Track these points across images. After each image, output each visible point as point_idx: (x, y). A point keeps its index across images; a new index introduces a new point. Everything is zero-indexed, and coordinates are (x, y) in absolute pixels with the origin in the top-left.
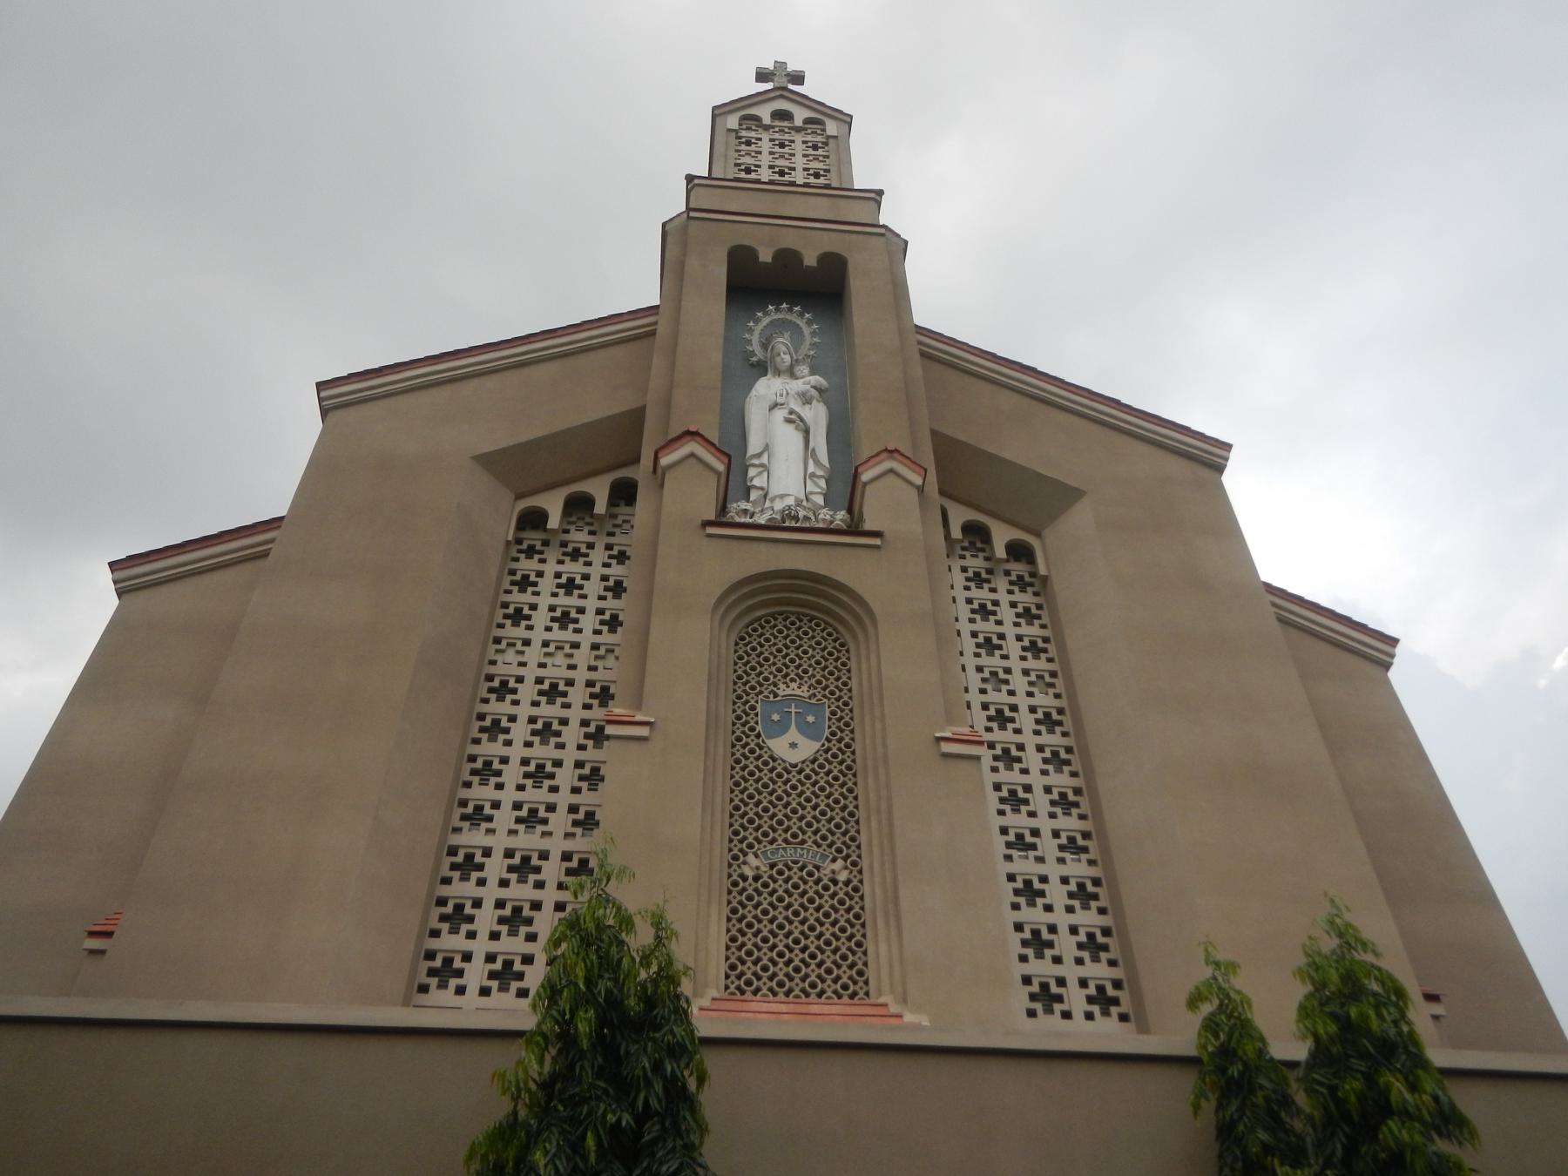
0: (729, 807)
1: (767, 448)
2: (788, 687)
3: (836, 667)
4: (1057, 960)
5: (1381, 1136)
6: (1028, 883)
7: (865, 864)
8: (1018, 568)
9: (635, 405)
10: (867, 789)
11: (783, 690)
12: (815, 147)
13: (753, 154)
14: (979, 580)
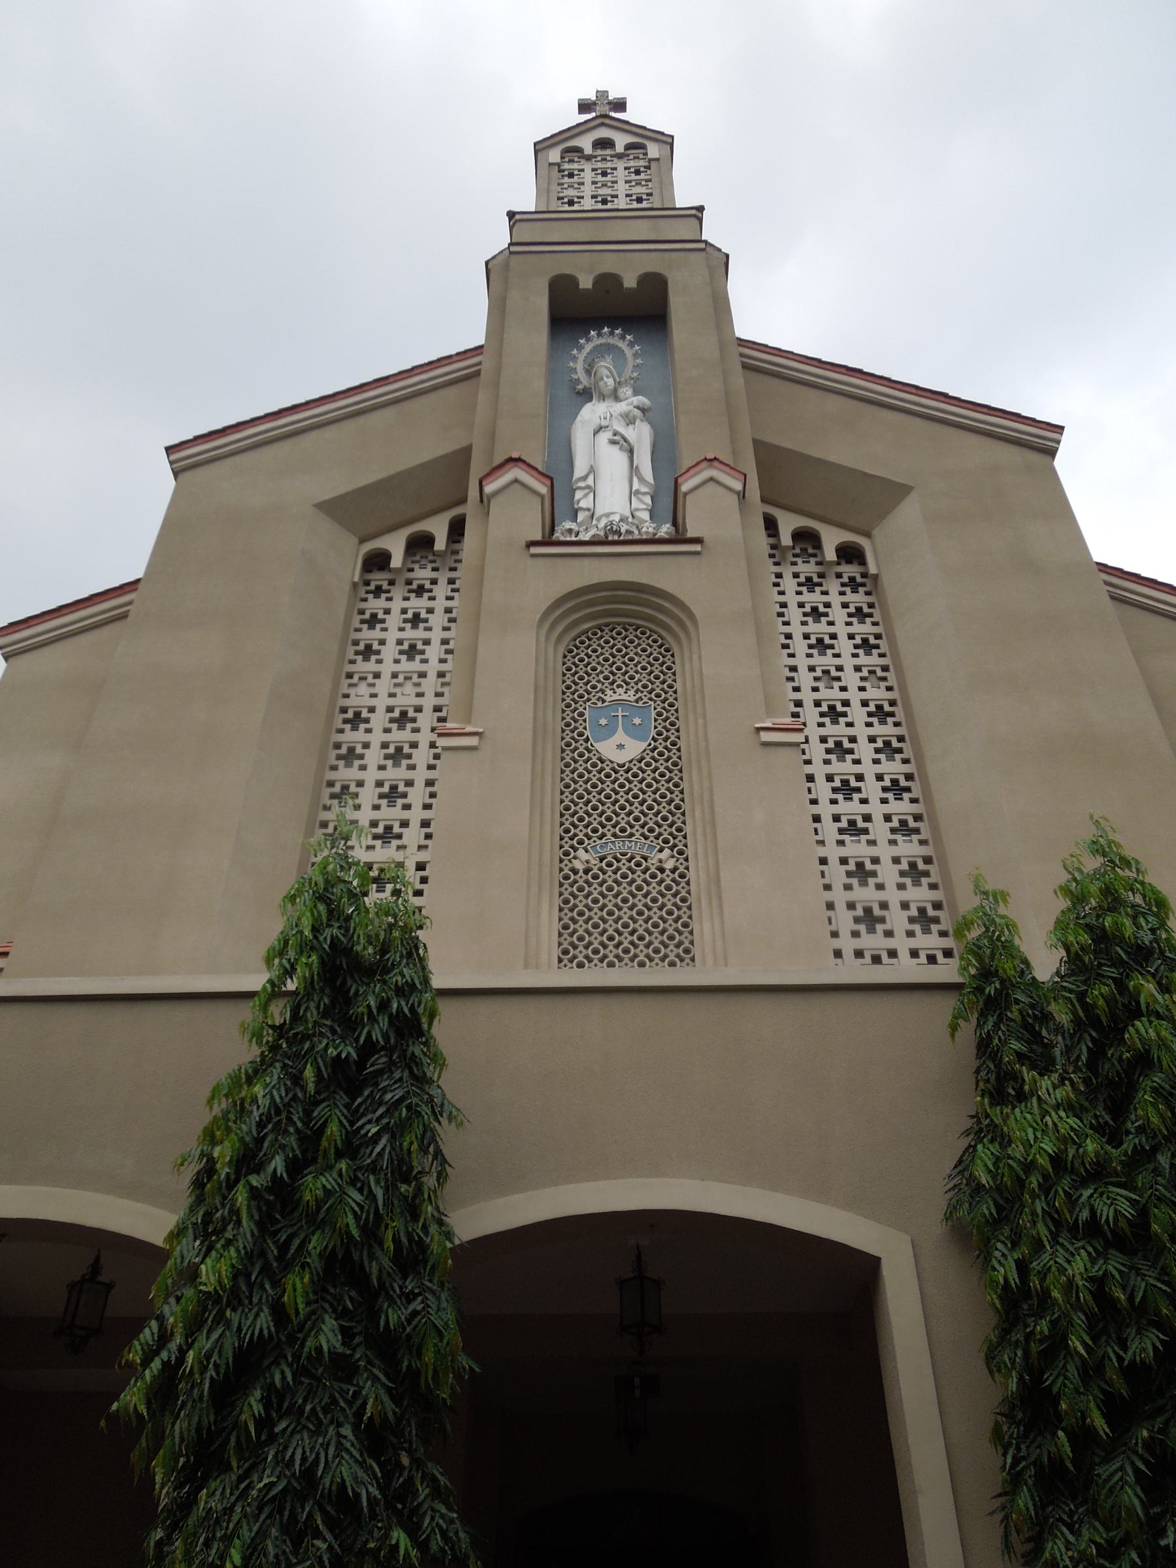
0: (559, 808)
1: (592, 470)
2: (615, 693)
3: (662, 672)
4: (889, 934)
5: (1127, 1036)
6: (860, 865)
7: (690, 852)
8: (850, 570)
9: (464, 444)
10: (692, 782)
11: (610, 696)
12: (637, 172)
13: (576, 186)
14: (810, 584)
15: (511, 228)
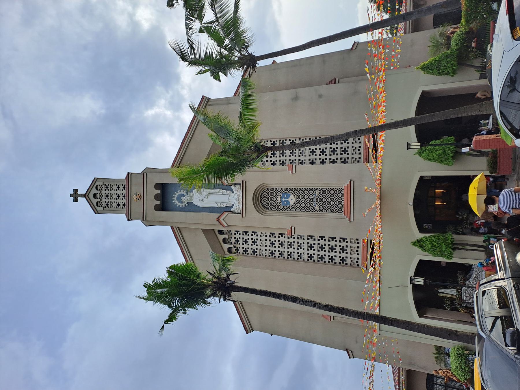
7: (316, 188)
15: (132, 220)
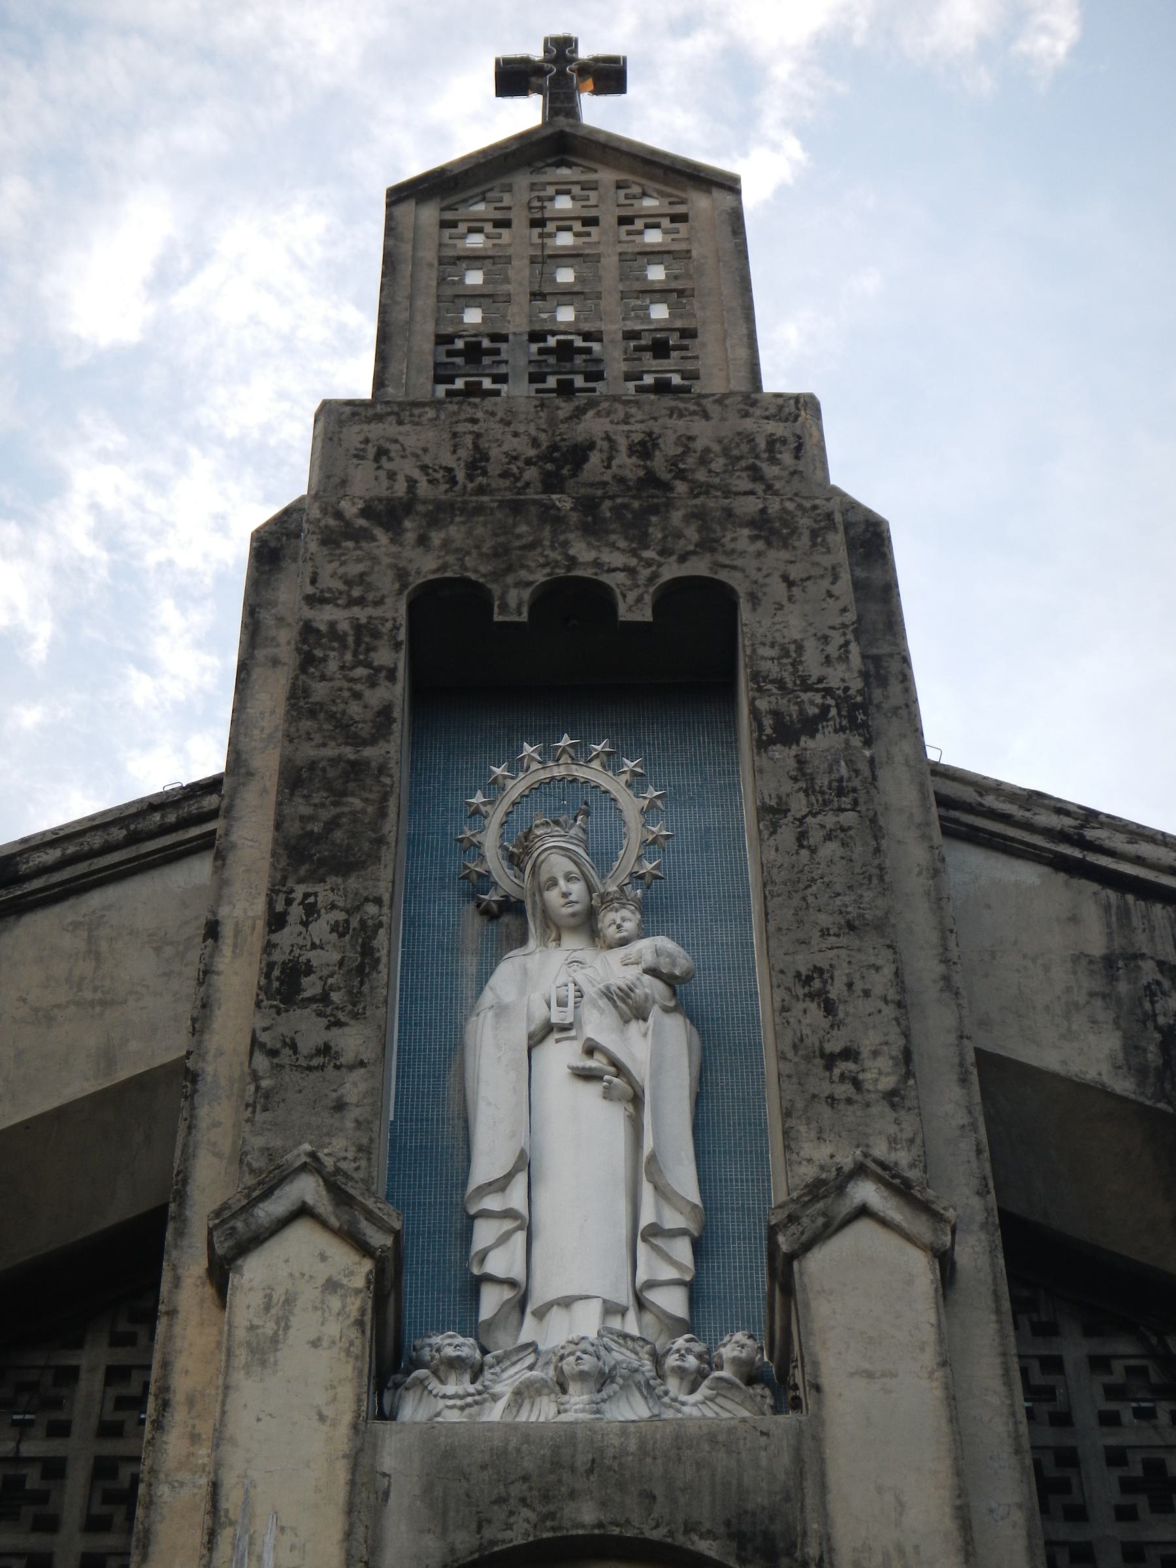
1: (525, 1163)
